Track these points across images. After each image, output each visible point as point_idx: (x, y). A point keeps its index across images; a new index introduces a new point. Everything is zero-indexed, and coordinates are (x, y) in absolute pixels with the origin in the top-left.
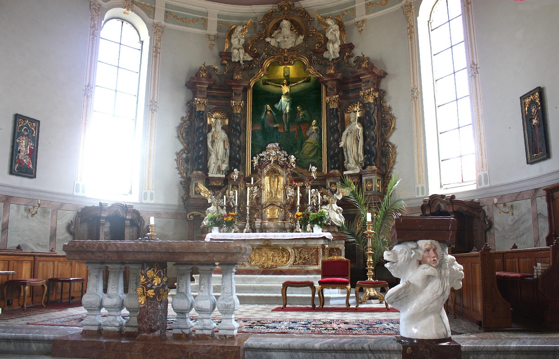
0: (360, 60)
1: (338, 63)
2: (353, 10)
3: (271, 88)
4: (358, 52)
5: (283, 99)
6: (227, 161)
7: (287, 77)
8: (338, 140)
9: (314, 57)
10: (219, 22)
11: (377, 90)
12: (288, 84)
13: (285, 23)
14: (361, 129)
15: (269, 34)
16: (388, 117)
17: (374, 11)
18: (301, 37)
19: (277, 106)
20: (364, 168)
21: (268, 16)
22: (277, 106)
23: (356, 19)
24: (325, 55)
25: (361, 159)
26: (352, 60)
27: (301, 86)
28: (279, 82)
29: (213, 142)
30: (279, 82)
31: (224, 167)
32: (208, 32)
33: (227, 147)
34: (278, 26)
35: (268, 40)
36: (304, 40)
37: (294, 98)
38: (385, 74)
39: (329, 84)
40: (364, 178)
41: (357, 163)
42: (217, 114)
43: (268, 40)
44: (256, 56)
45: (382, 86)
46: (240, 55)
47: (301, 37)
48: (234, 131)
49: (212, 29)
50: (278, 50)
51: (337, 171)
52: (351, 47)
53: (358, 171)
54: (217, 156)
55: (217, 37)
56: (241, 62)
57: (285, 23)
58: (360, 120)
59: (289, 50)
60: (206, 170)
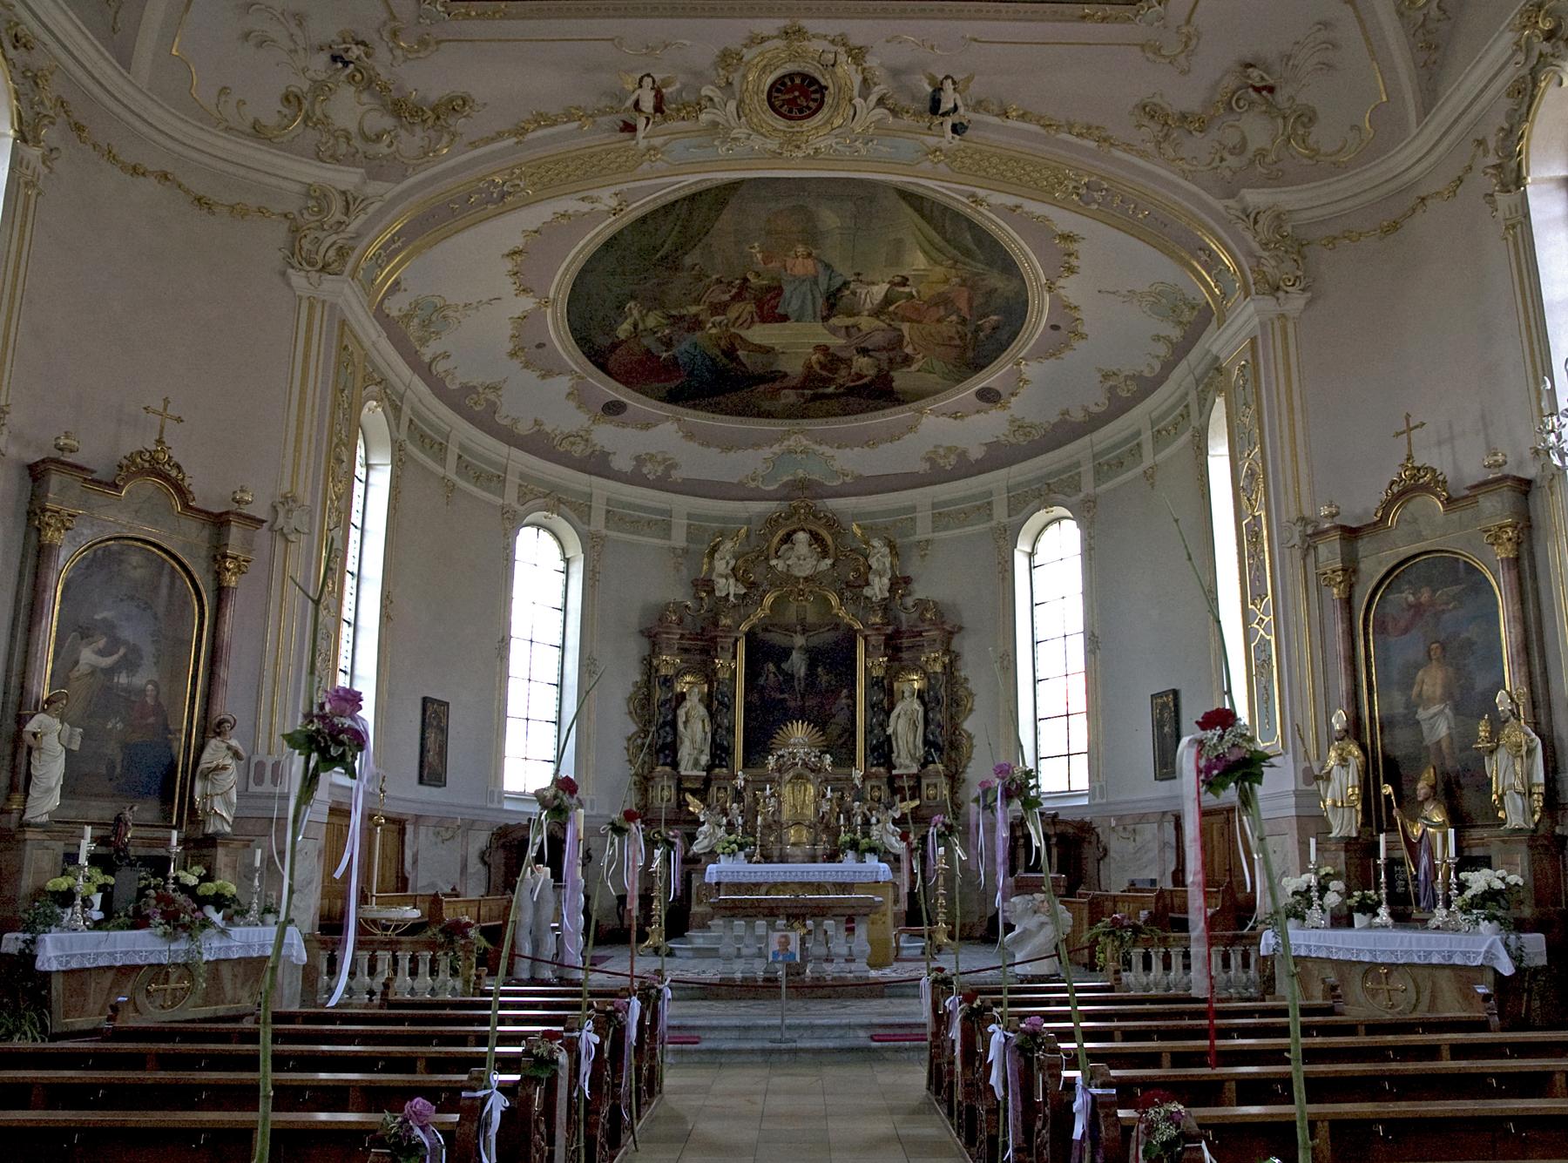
0: (922, 605)
1: (886, 606)
2: (913, 520)
3: (777, 638)
4: (920, 591)
5: (795, 655)
6: (707, 750)
7: (802, 622)
8: (883, 725)
9: (848, 594)
10: (689, 526)
11: (947, 651)
12: (804, 631)
13: (802, 537)
14: (921, 710)
15: (772, 551)
16: (962, 692)
17: (946, 528)
18: (829, 562)
19: (784, 666)
20: (924, 765)
21: (772, 522)
22: (784, 666)
23: (917, 538)
24: (867, 592)
25: (920, 752)
26: (909, 601)
27: (825, 638)
28: (788, 630)
29: (685, 723)
30: (788, 630)
31: (704, 759)
32: (673, 543)
33: (708, 729)
34: (788, 538)
35: (773, 562)
36: (833, 565)
37: (814, 657)
38: (961, 628)
39: (873, 640)
40: (924, 783)
41: (913, 757)
42: (688, 678)
43: (773, 562)
44: (752, 585)
45: (955, 645)
46: (727, 587)
47: (829, 562)
48: (716, 704)
49: (679, 539)
50: (788, 578)
51: (882, 770)
52: (907, 580)
53: (914, 770)
54: (693, 742)
55: (686, 551)
56: (732, 598)
57: (802, 537)
58: (920, 695)
59: (806, 579)
60: (675, 765)
